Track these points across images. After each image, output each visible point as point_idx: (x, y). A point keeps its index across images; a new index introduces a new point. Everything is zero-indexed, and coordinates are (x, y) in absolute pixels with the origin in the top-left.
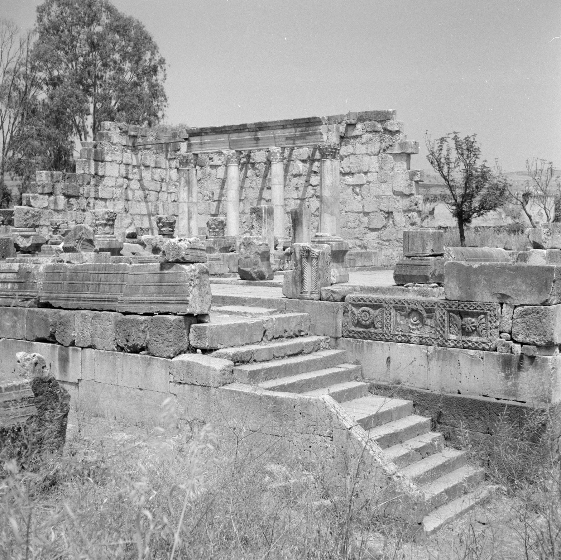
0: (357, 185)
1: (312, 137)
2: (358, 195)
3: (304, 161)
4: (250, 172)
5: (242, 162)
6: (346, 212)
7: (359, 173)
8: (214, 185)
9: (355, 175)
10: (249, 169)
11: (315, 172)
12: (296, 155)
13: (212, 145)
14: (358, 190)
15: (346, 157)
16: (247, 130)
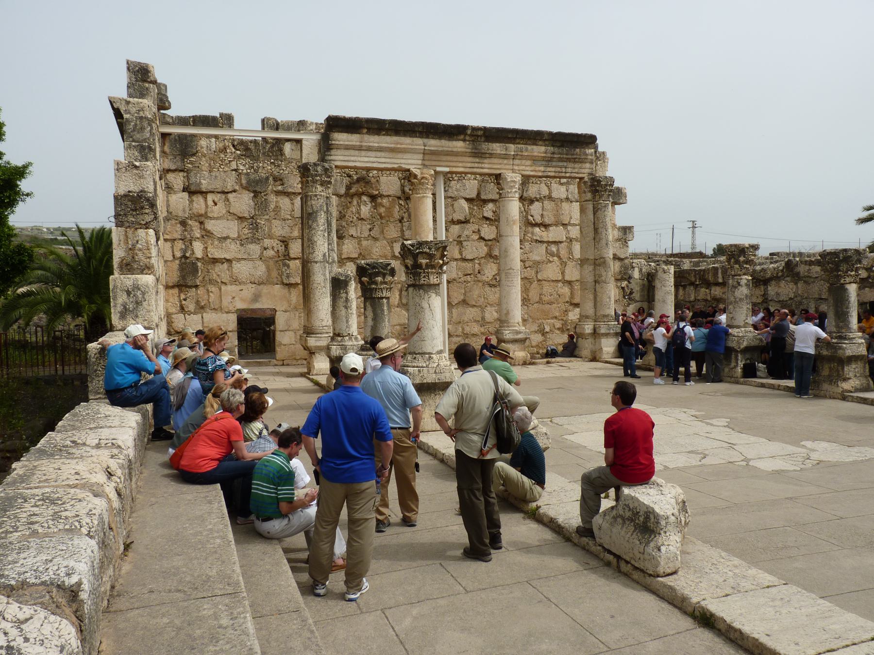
0: (554, 242)
1: (576, 166)
2: (552, 255)
3: (469, 200)
4: (366, 210)
5: (353, 190)
6: (539, 280)
7: (556, 225)
8: (287, 229)
9: (551, 228)
10: (365, 204)
11: (487, 219)
12: (457, 190)
13: (383, 154)
14: (554, 248)
15: (537, 200)
16: (462, 137)
